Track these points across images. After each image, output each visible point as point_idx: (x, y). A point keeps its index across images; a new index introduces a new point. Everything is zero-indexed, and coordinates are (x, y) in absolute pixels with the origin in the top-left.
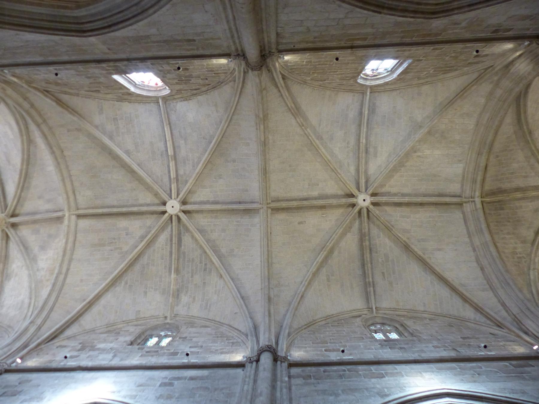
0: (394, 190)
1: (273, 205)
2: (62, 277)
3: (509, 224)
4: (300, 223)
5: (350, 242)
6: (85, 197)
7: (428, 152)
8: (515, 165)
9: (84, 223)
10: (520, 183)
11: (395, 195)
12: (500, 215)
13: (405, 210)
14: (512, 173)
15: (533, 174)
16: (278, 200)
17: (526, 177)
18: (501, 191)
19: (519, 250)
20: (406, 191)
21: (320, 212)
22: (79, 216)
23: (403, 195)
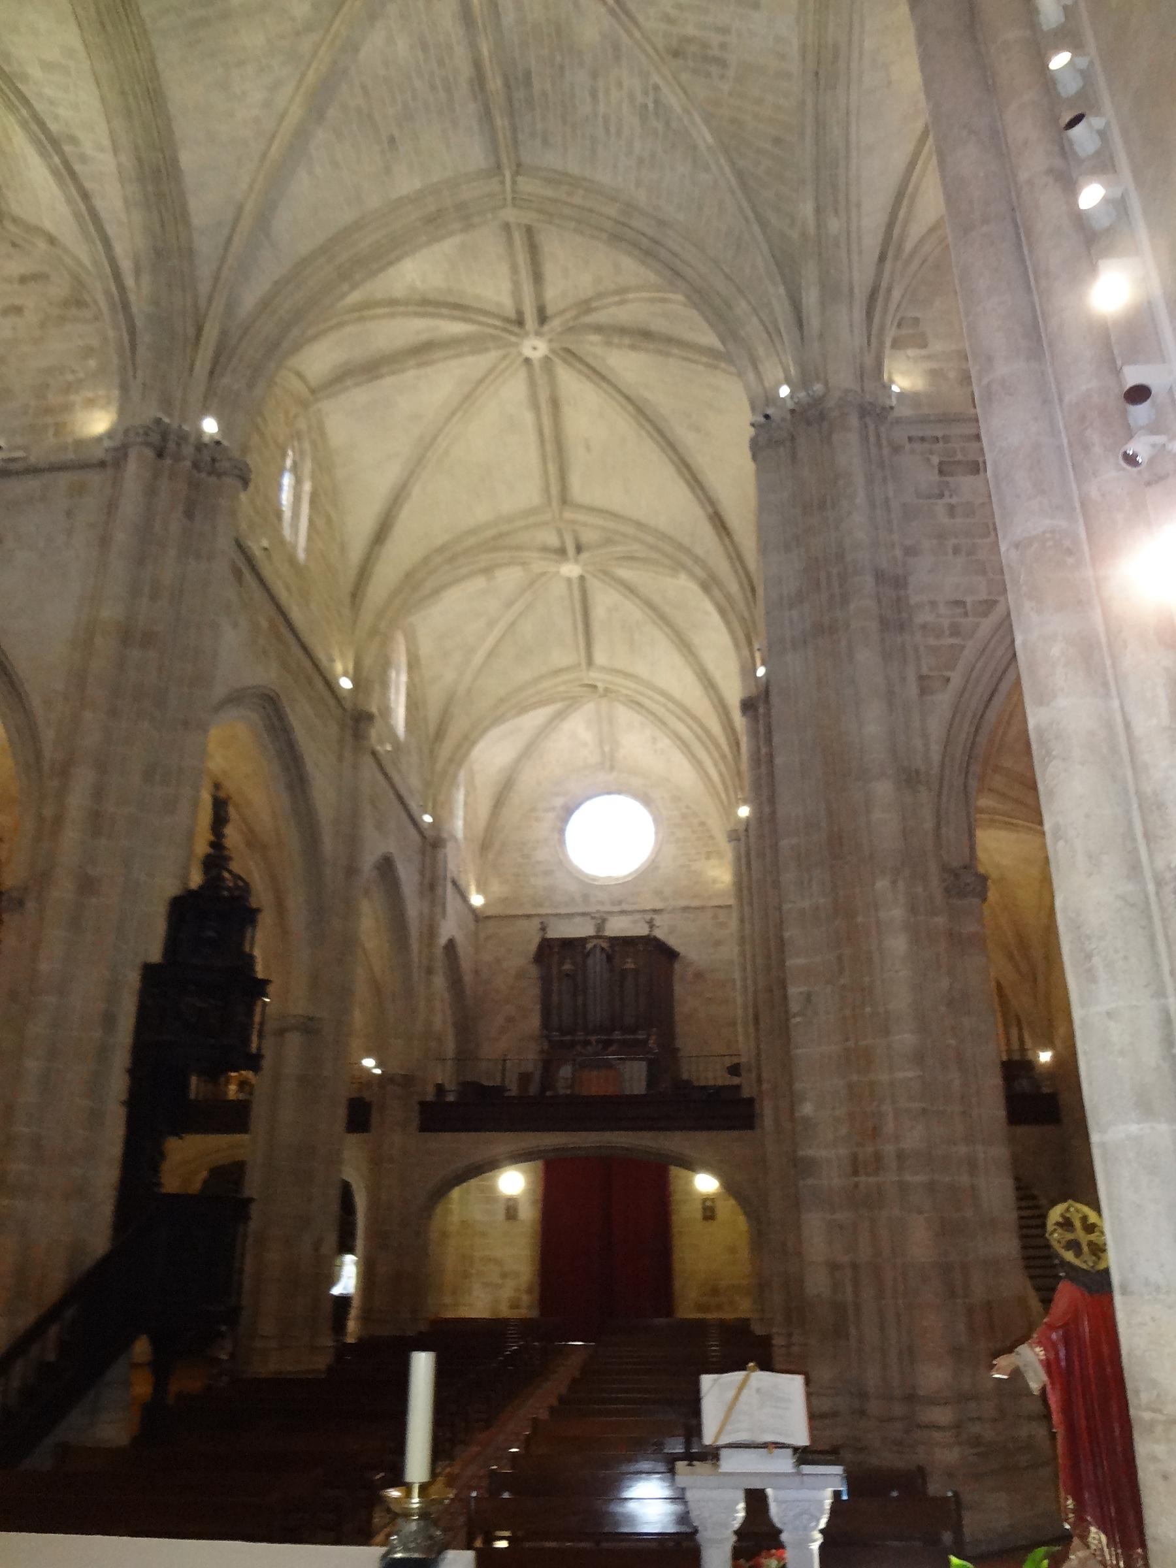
0: (506, 286)
1: (555, 503)
2: (670, 705)
4: (588, 448)
5: (627, 364)
6: (563, 656)
8: (402, 46)
9: (600, 658)
11: (516, 284)
12: (544, 94)
14: (425, 47)
16: (547, 489)
21: (567, 411)
22: (590, 662)
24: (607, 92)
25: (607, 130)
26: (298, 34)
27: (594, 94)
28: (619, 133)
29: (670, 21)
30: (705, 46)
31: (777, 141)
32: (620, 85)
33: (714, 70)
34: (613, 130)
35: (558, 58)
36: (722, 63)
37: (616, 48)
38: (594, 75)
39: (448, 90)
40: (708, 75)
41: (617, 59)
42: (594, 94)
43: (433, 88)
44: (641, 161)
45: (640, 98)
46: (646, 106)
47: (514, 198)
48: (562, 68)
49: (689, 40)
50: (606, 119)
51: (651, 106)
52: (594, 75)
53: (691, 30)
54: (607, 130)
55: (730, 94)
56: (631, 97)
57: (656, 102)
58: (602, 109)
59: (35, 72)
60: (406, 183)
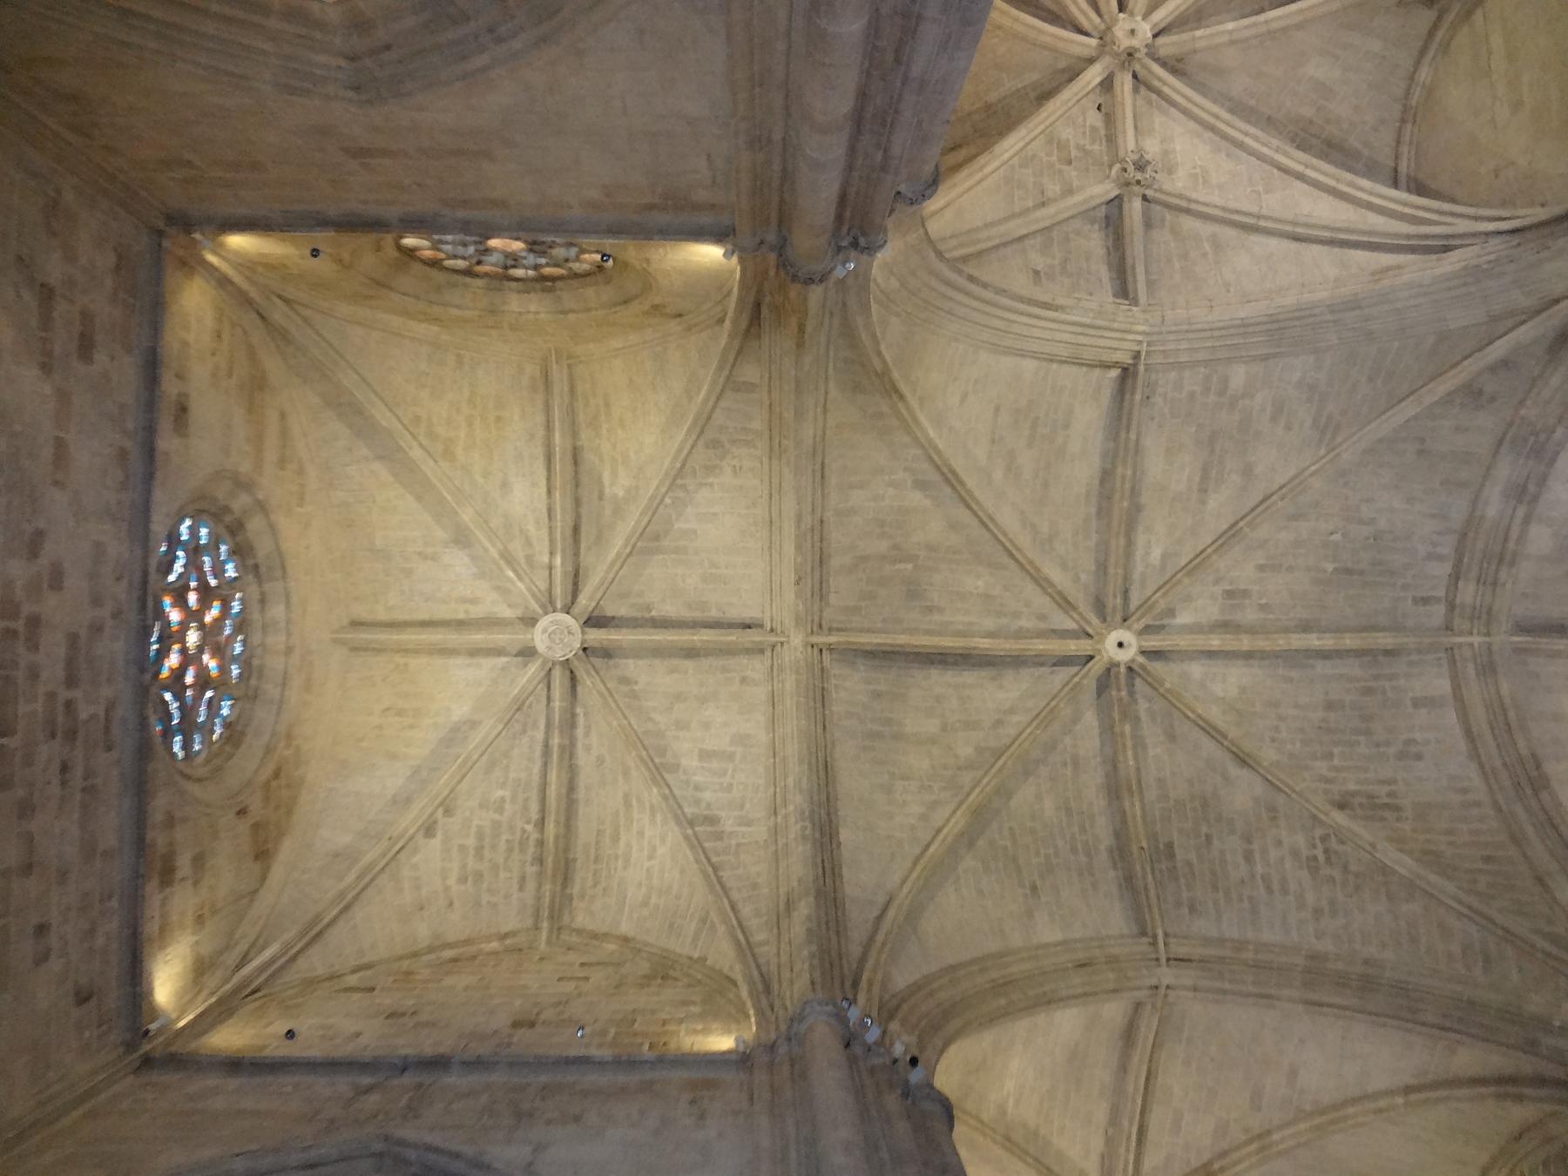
0: (1097, 1144)
3: (1215, 842)
7: (1010, 1085)
8: (1048, 804)
10: (1092, 781)
11: (1110, 1141)
12: (1189, 864)
13: (1159, 1118)
14: (1068, 811)
15: (1068, 740)
17: (1076, 763)
18: (1121, 851)
19: (1300, 840)
20: (1101, 1114)
23: (1114, 1119)
24: (1264, 851)
25: (1269, 890)
26: (959, 768)
27: (1249, 857)
28: (1285, 892)
29: (1328, 781)
30: (1371, 797)
31: (1488, 859)
32: (1279, 843)
33: (1387, 814)
34: (1276, 886)
35: (1204, 829)
36: (1398, 808)
37: (1272, 809)
38: (1248, 840)
39: (1088, 855)
40: (1383, 819)
41: (1274, 819)
42: (1249, 857)
43: (1074, 850)
44: (1318, 912)
45: (1305, 852)
46: (1315, 858)
47: (1168, 960)
48: (1208, 838)
49: (1353, 794)
50: (1266, 879)
51: (1321, 858)
52: (1248, 840)
53: (1352, 787)
54: (1269, 890)
55: (1414, 830)
56: (1295, 854)
57: (1326, 851)
58: (1259, 869)
59: (691, 762)
60: (1048, 933)
